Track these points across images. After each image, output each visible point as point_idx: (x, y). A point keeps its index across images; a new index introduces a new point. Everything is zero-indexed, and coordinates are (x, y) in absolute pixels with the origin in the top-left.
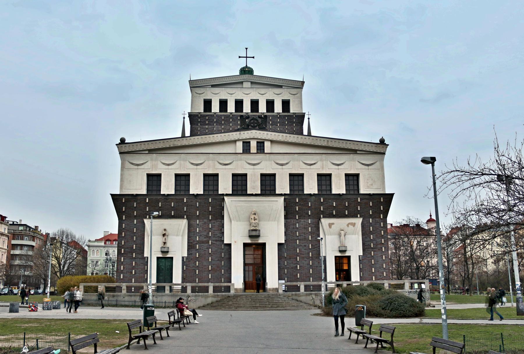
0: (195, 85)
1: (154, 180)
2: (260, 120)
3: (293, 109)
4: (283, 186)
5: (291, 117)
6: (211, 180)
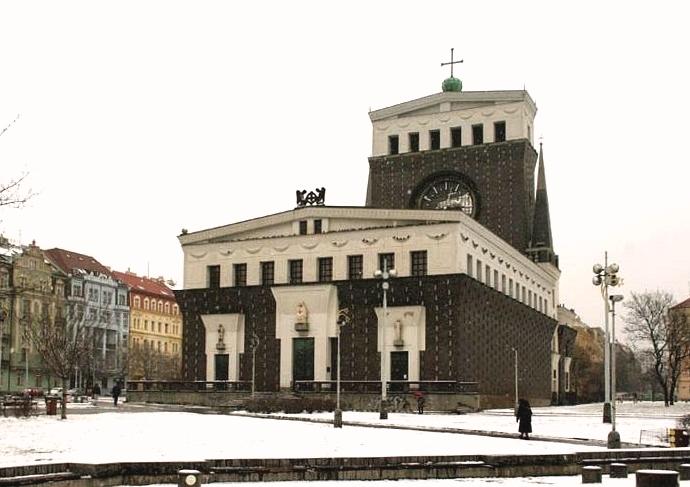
0: (377, 117)
1: (214, 271)
2: (317, 194)
3: (511, 134)
4: (340, 272)
5: (505, 147)
6: (267, 268)
